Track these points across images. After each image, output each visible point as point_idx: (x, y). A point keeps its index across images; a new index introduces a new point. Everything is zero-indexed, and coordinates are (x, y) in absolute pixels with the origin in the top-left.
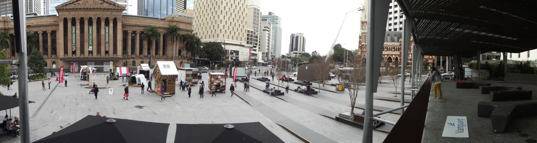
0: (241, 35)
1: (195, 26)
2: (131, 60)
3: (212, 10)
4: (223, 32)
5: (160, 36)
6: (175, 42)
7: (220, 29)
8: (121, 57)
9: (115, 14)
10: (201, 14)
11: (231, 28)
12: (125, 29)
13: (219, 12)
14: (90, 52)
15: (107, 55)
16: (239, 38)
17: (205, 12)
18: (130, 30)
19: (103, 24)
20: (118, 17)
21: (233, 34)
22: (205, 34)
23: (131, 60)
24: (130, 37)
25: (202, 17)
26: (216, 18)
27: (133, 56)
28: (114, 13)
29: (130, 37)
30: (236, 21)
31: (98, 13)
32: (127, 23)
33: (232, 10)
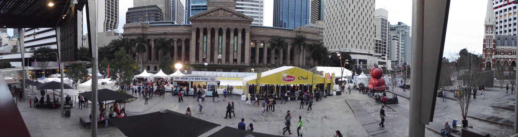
0: (369, 45)
1: (326, 36)
3: (341, 22)
4: (351, 43)
5: (287, 46)
6: (302, 52)
7: (348, 39)
8: (248, 65)
9: (244, 25)
10: (331, 25)
11: (359, 38)
13: (347, 24)
14: (220, 60)
15: (235, 63)
16: (367, 48)
17: (334, 24)
19: (232, 34)
20: (246, 28)
21: (361, 44)
25: (332, 28)
26: (345, 29)
27: (260, 64)
28: (242, 24)
31: (228, 24)
32: (255, 33)
33: (359, 21)
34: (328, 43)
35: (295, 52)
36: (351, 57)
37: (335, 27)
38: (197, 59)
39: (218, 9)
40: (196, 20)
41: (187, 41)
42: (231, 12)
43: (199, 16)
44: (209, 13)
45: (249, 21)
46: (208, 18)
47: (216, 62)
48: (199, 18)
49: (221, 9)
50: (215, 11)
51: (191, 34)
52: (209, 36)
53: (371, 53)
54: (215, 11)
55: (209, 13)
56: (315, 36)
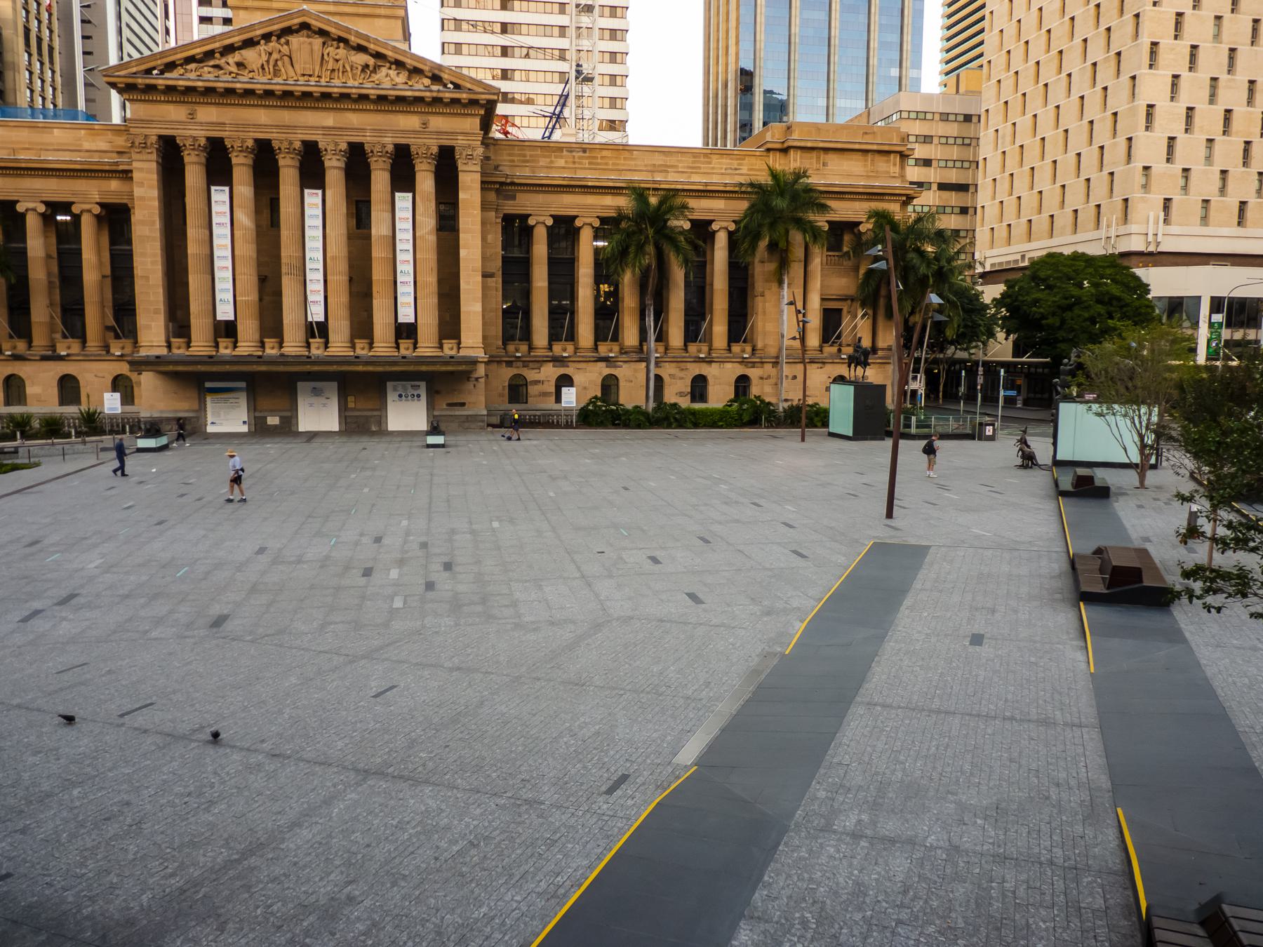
2: (550, 373)
5: (712, 236)
6: (797, 269)
7: (1138, 164)
8: (480, 354)
10: (1027, 85)
12: (511, 207)
13: (1136, 60)
14: (319, 330)
15: (405, 344)
17: (1048, 74)
18: (541, 211)
19: (380, 179)
20: (460, 142)
22: (1051, 204)
23: (550, 373)
24: (540, 250)
26: (1119, 100)
27: (557, 348)
28: (439, 123)
29: (540, 250)
31: (354, 119)
32: (522, 173)
34: (1010, 202)
35: (761, 267)
36: (1145, 288)
37: (1057, 95)
38: (179, 324)
39: (287, 31)
40: (151, 88)
41: (116, 219)
42: (360, 49)
43: (171, 66)
44: (229, 49)
45: (473, 103)
46: (223, 81)
47: (293, 344)
48: (173, 78)
49: (305, 26)
50: (267, 37)
51: (126, 175)
52: (244, 187)
54: (267, 37)
55: (229, 49)
56: (882, 165)
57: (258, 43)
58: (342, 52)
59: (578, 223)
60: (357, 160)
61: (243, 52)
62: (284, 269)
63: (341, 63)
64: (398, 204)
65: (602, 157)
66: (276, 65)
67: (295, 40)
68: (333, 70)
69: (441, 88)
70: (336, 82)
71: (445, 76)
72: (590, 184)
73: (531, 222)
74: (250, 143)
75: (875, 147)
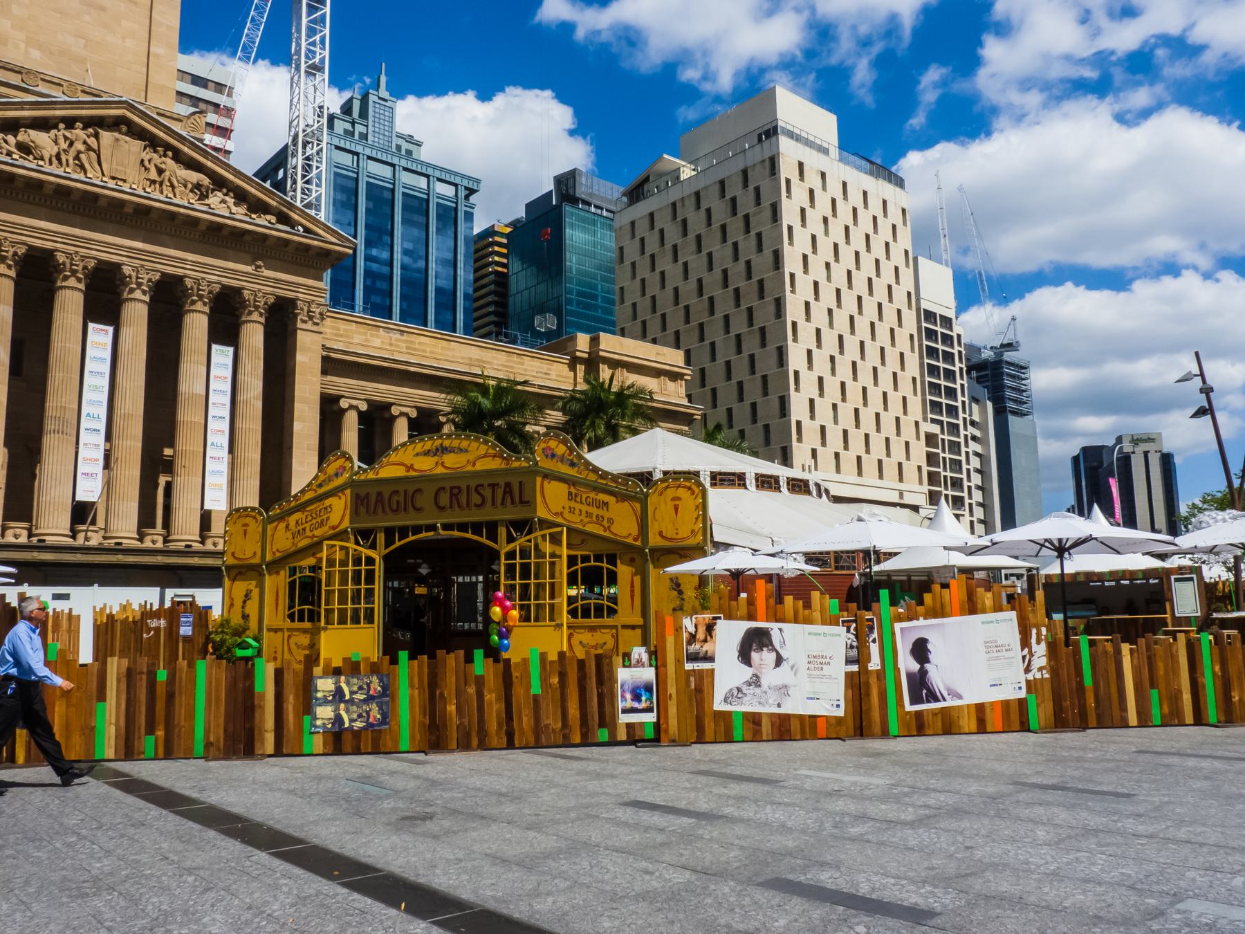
0: (898, 452)
3: (739, 325)
11: (846, 412)
19: (196, 324)
30: (865, 378)
50: (70, 123)
53: (908, 499)
54: (70, 123)
57: (56, 127)
58: (169, 164)
59: (395, 411)
60: (168, 300)
61: (30, 131)
62: (49, 425)
63: (167, 173)
64: (215, 359)
65: (420, 343)
66: (77, 158)
67: (107, 137)
68: (153, 182)
69: (288, 229)
70: (157, 195)
71: (296, 217)
72: (412, 369)
73: (344, 404)
74: (21, 250)
75: (667, 368)
